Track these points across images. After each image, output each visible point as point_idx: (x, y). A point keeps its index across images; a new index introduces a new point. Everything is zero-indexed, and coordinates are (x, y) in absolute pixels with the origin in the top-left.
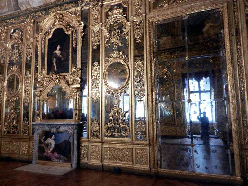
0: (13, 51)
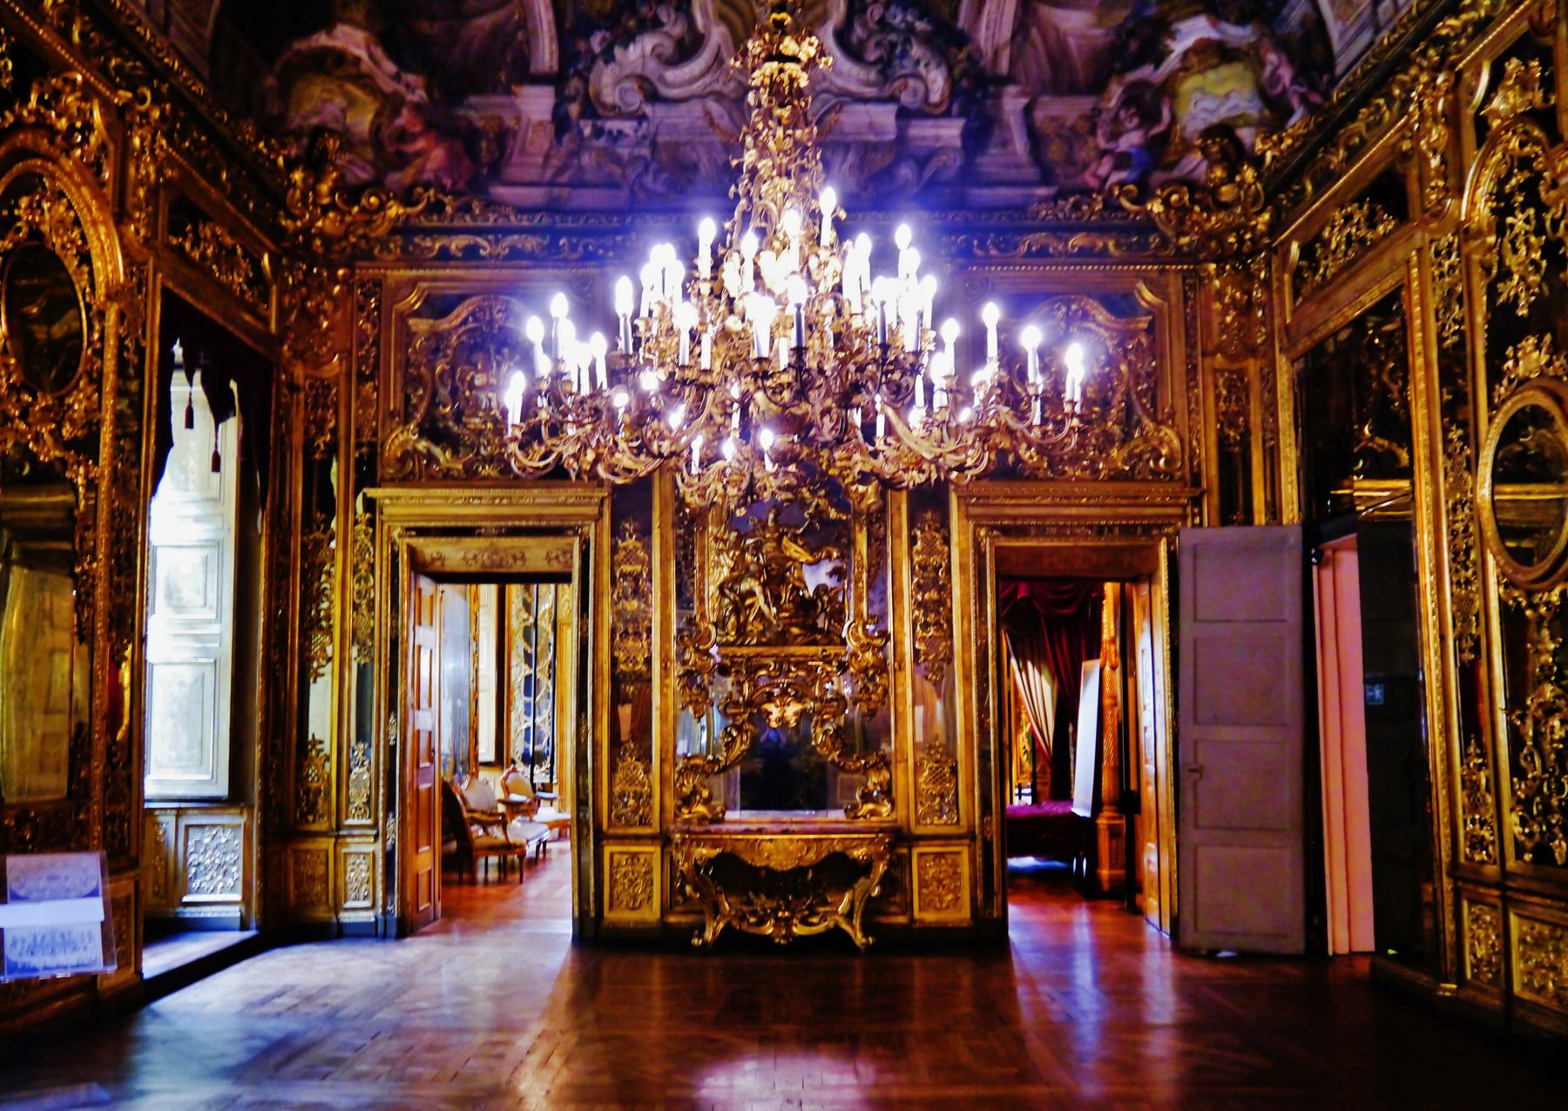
0: (1501, 229)
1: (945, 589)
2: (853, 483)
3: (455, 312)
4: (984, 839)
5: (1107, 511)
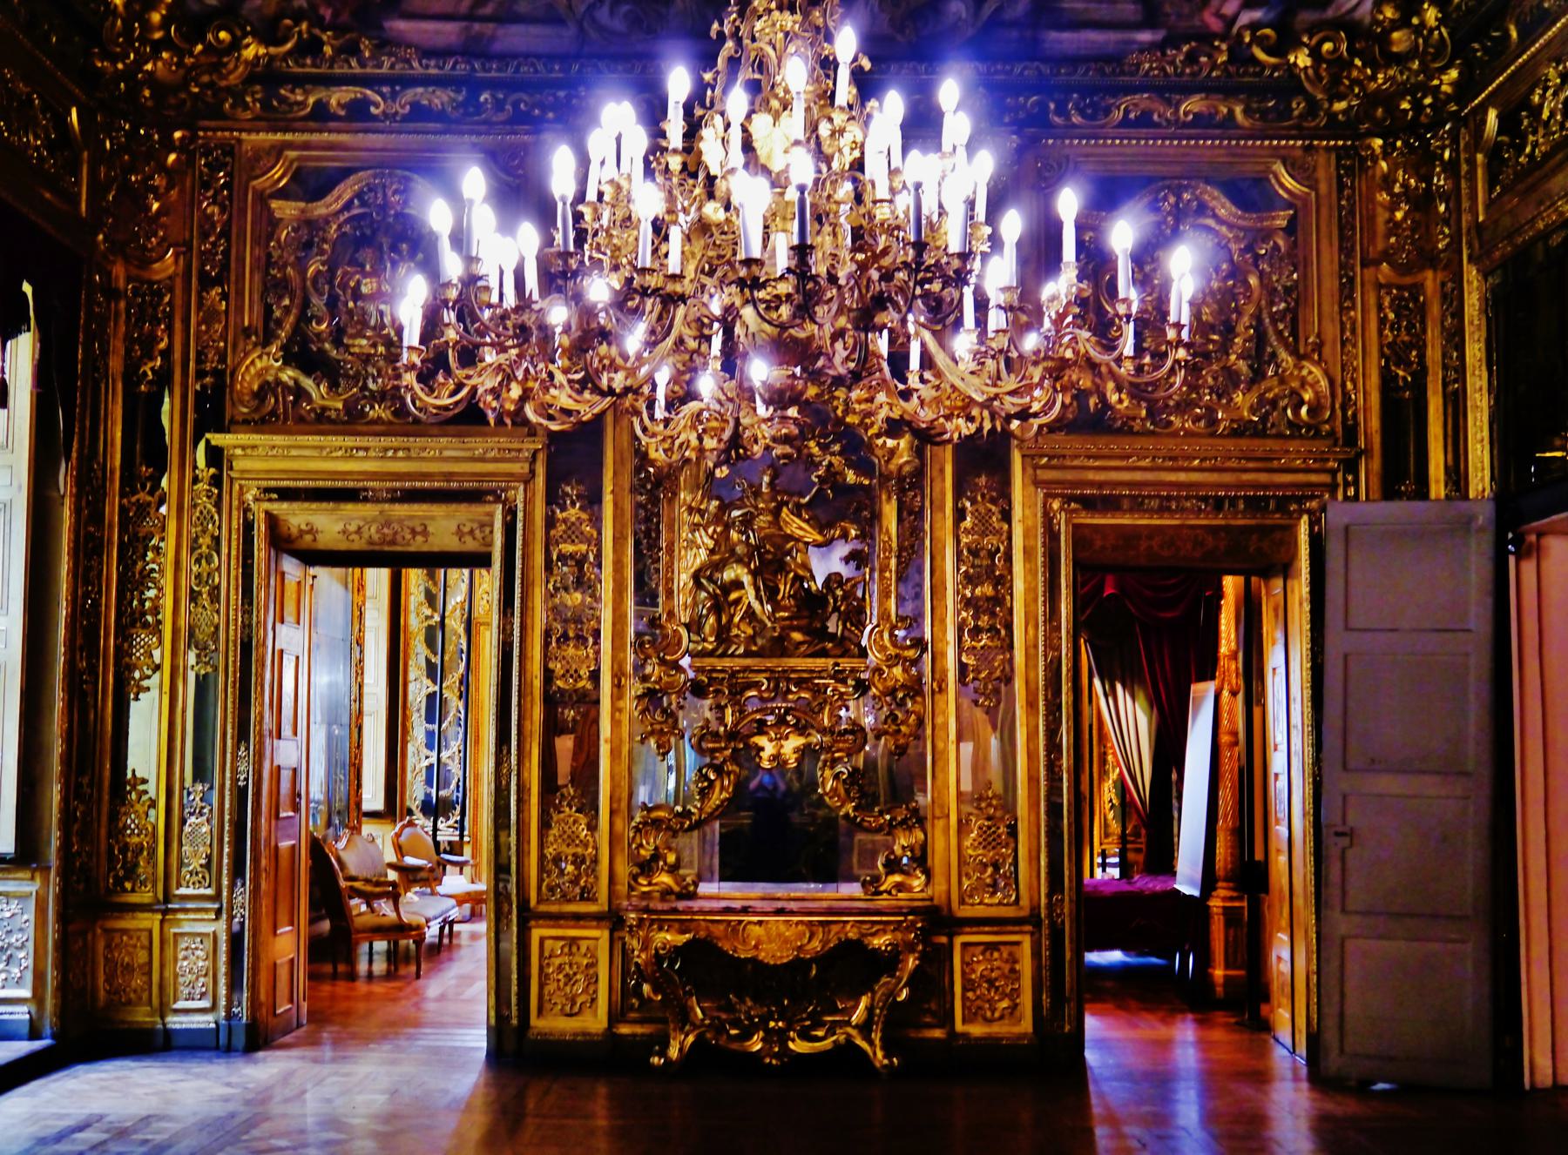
1: (1003, 581)
2: (878, 436)
3: (336, 192)
4: (1053, 924)
5: (1227, 478)
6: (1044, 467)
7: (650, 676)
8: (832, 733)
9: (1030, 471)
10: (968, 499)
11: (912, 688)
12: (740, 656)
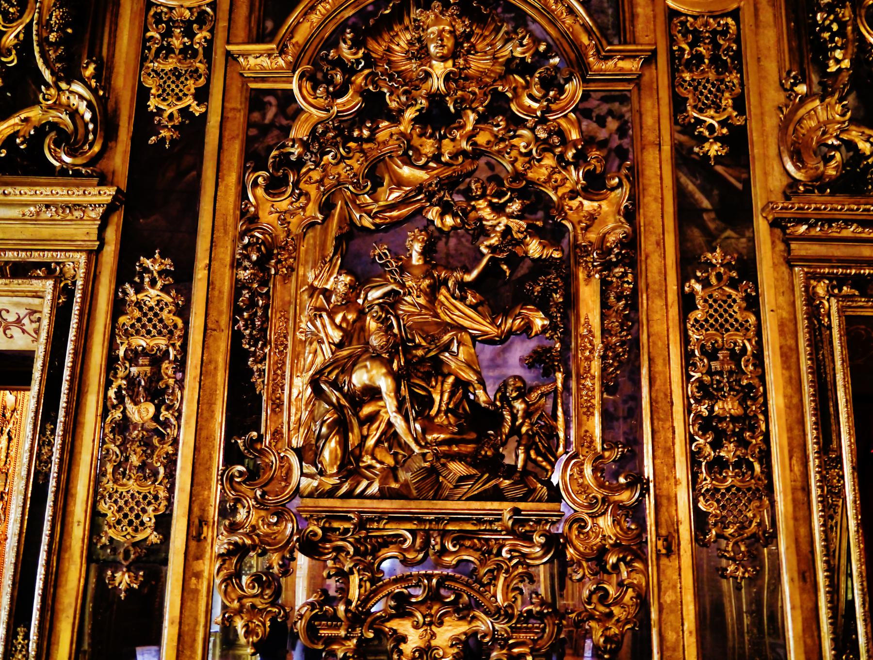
1: (752, 394)
2: (573, 194)
6: (802, 238)
7: (241, 525)
8: (510, 617)
9: (781, 247)
10: (698, 280)
11: (626, 549)
12: (372, 497)
